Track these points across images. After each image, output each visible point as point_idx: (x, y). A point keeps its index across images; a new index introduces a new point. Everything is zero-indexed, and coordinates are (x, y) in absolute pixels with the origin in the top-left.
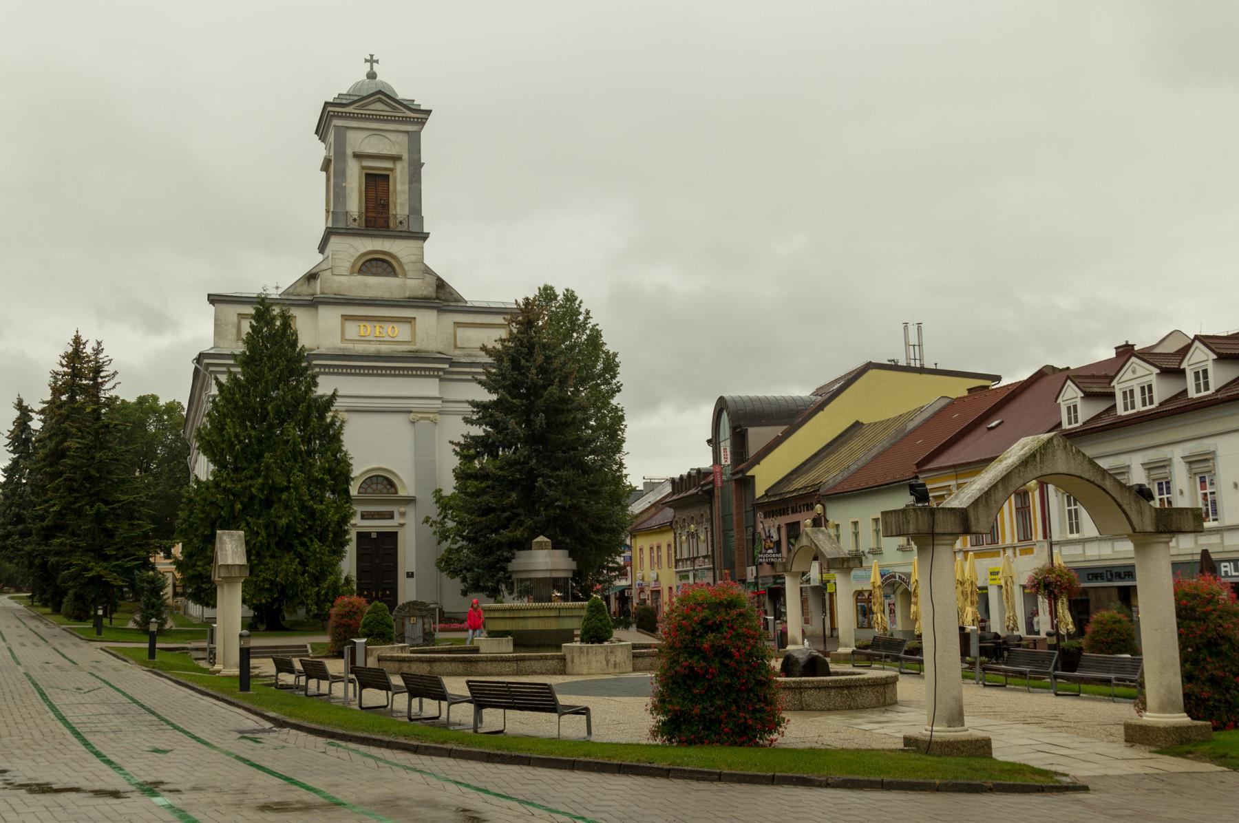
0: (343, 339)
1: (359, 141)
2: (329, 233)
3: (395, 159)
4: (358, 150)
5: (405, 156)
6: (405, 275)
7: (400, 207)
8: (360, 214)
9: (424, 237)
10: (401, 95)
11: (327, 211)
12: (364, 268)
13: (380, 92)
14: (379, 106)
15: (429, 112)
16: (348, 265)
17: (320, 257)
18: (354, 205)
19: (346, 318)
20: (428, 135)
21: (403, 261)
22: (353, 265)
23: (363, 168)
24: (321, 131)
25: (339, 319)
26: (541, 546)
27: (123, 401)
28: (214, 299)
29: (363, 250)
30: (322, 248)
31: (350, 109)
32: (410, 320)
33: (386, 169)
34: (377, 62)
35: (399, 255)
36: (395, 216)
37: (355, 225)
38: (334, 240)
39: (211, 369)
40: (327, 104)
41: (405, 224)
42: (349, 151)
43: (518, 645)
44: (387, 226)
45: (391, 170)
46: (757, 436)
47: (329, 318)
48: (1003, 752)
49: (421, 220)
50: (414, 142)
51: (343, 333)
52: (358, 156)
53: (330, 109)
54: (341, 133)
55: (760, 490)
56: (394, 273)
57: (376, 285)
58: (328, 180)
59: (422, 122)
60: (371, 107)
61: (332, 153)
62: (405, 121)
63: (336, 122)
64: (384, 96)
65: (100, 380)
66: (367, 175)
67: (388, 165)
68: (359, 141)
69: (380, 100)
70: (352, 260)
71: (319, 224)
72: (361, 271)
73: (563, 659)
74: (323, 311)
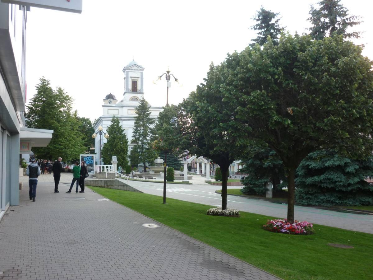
0: (128, 114)
1: (132, 74)
2: (125, 93)
3: (138, 78)
4: (131, 76)
7: (139, 87)
8: (131, 89)
10: (139, 65)
11: (125, 88)
14: (135, 67)
17: (123, 97)
18: (130, 87)
20: (144, 72)
22: (130, 99)
23: (132, 80)
24: (124, 70)
25: (127, 110)
26: (159, 158)
30: (124, 94)
31: (129, 68)
36: (138, 89)
37: (130, 91)
38: (126, 94)
39: (103, 120)
42: (129, 76)
43: (155, 172)
44: (136, 91)
47: (125, 109)
48: (190, 182)
49: (143, 90)
50: (142, 74)
51: (128, 113)
54: (127, 72)
58: (125, 81)
60: (134, 67)
61: (126, 77)
62: (140, 70)
64: (136, 65)
67: (137, 79)
68: (132, 74)
69: (135, 66)
71: (124, 91)
73: (160, 174)
74: (124, 108)
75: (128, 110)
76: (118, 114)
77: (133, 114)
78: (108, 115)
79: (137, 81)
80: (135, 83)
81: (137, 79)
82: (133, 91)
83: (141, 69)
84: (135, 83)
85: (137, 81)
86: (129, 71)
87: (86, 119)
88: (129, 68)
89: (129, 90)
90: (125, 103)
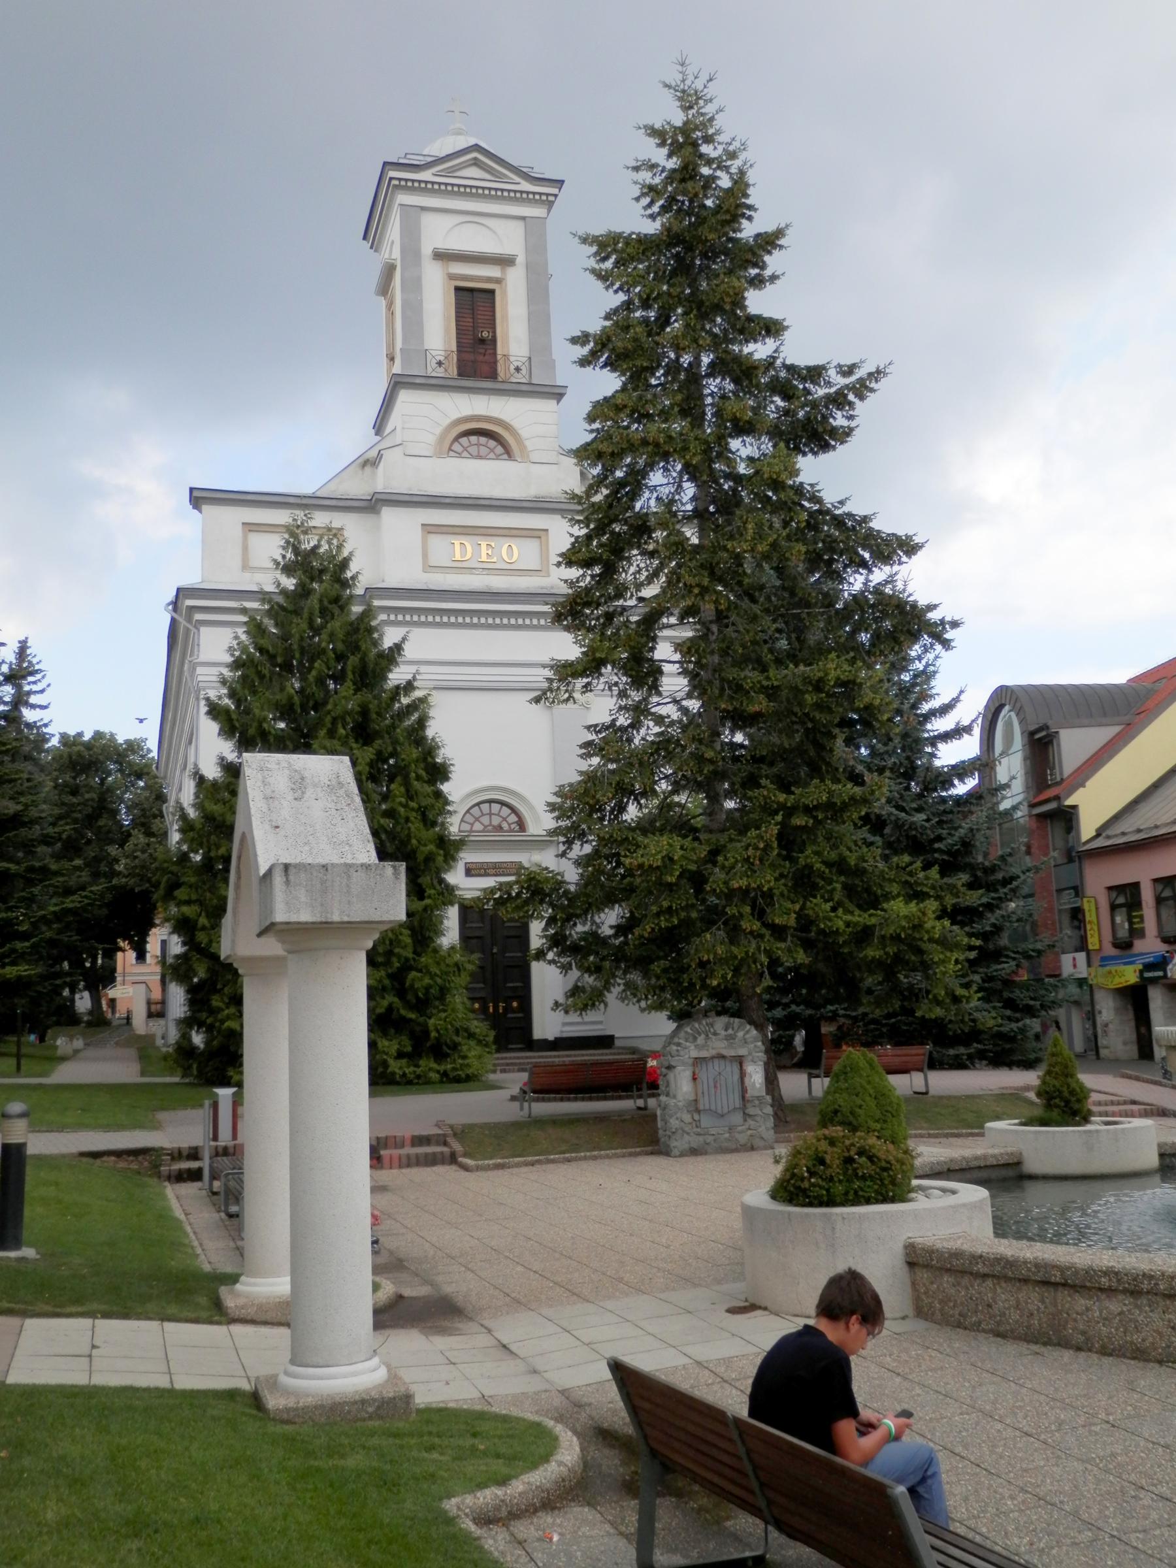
0: (428, 567)
1: (443, 230)
3: (505, 261)
5: (521, 260)
6: (526, 458)
12: (456, 447)
13: (476, 148)
14: (474, 172)
15: (560, 183)
16: (431, 439)
21: (524, 433)
23: (452, 277)
27: (64, 737)
28: (199, 498)
29: (456, 415)
32: (538, 534)
33: (489, 280)
35: (516, 424)
37: (440, 372)
38: (405, 398)
39: (198, 616)
40: (385, 164)
41: (524, 371)
42: (427, 250)
44: (493, 375)
45: (498, 281)
46: (1074, 744)
47: (400, 526)
51: (425, 555)
52: (441, 256)
53: (392, 174)
55: (1087, 828)
56: (508, 453)
63: (403, 198)
65: (27, 688)
66: (458, 289)
67: (493, 272)
68: (443, 230)
69: (476, 163)
70: (438, 431)
74: (387, 513)
75: (429, 529)
77: (471, 570)
78: (247, 575)
79: (492, 292)
82: (462, 374)
83: (526, 186)
85: (492, 292)
86: (423, 209)
87: (120, 740)
89: (433, 364)
90: (396, 475)
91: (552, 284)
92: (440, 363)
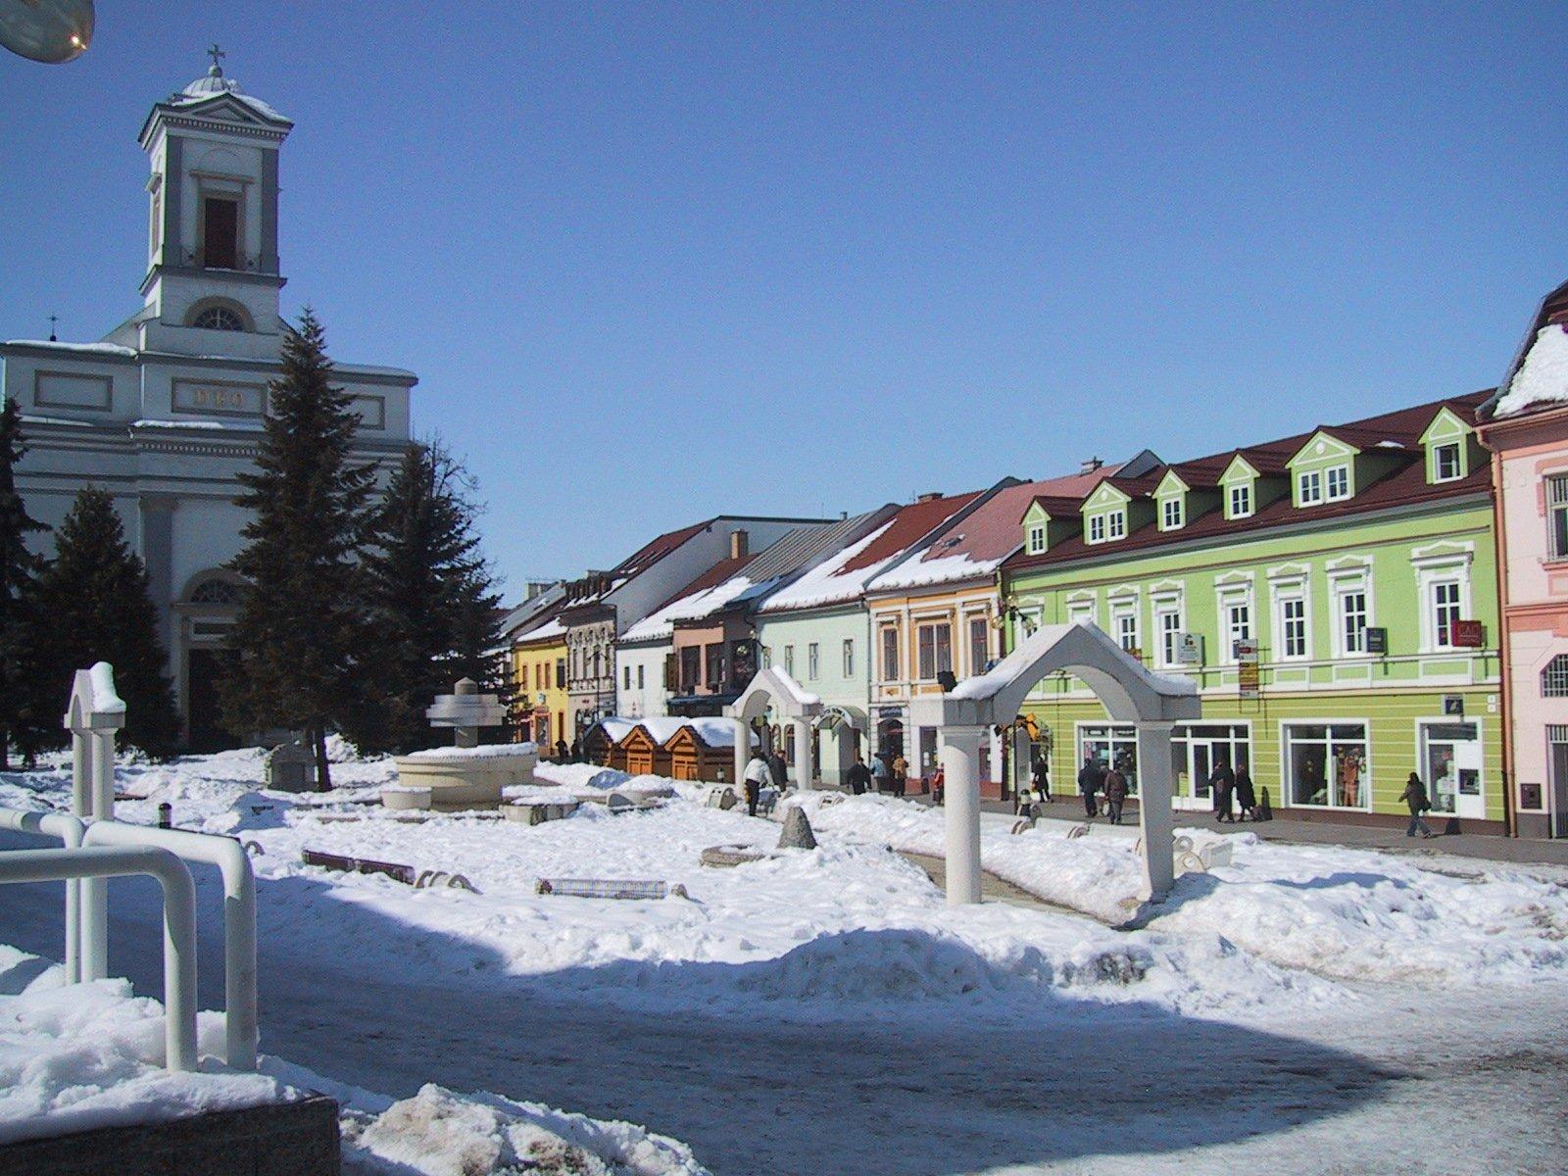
3: (246, 183)
5: (258, 178)
7: (251, 240)
8: (199, 249)
9: (282, 282)
14: (226, 112)
18: (191, 236)
19: (175, 382)
34: (222, 55)
36: (243, 254)
37: (191, 263)
50: (270, 161)
52: (198, 176)
56: (239, 329)
57: (216, 342)
59: (280, 138)
69: (227, 106)
72: (198, 325)
76: (108, 408)
79: (234, 204)
80: (221, 217)
81: (236, 188)
84: (221, 217)
85: (234, 204)
88: (183, 115)
91: (281, 196)
92: (191, 257)
